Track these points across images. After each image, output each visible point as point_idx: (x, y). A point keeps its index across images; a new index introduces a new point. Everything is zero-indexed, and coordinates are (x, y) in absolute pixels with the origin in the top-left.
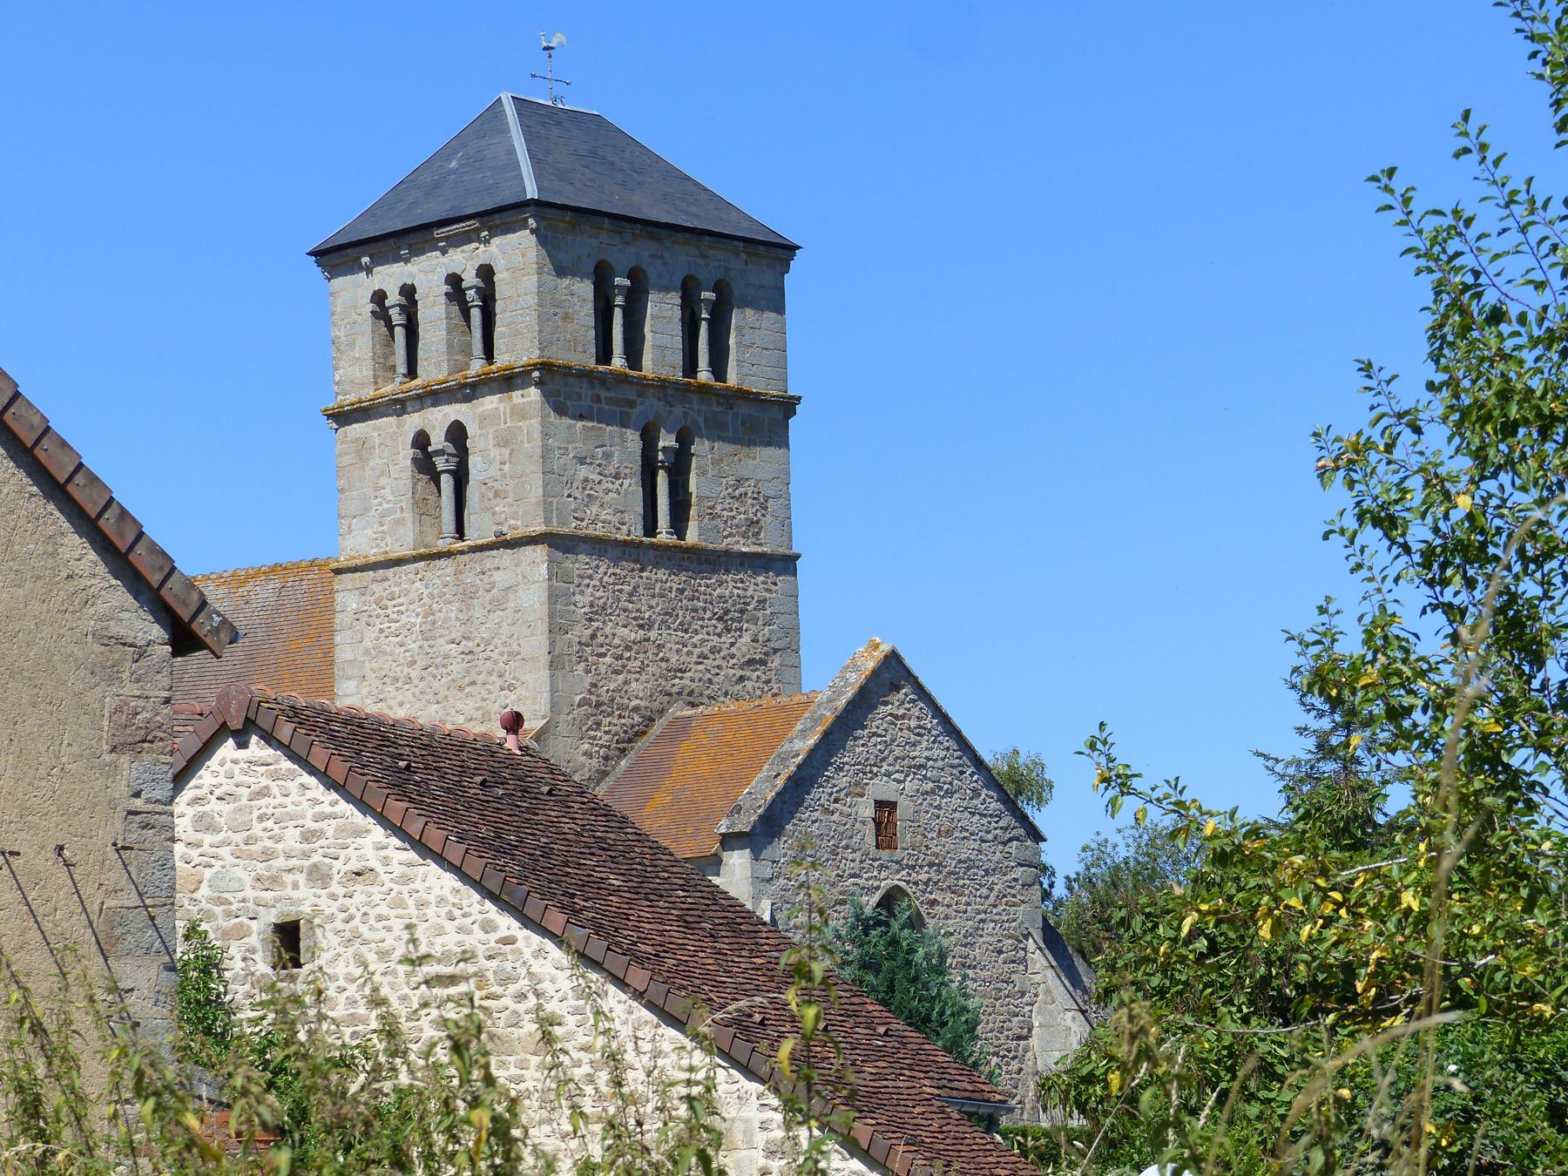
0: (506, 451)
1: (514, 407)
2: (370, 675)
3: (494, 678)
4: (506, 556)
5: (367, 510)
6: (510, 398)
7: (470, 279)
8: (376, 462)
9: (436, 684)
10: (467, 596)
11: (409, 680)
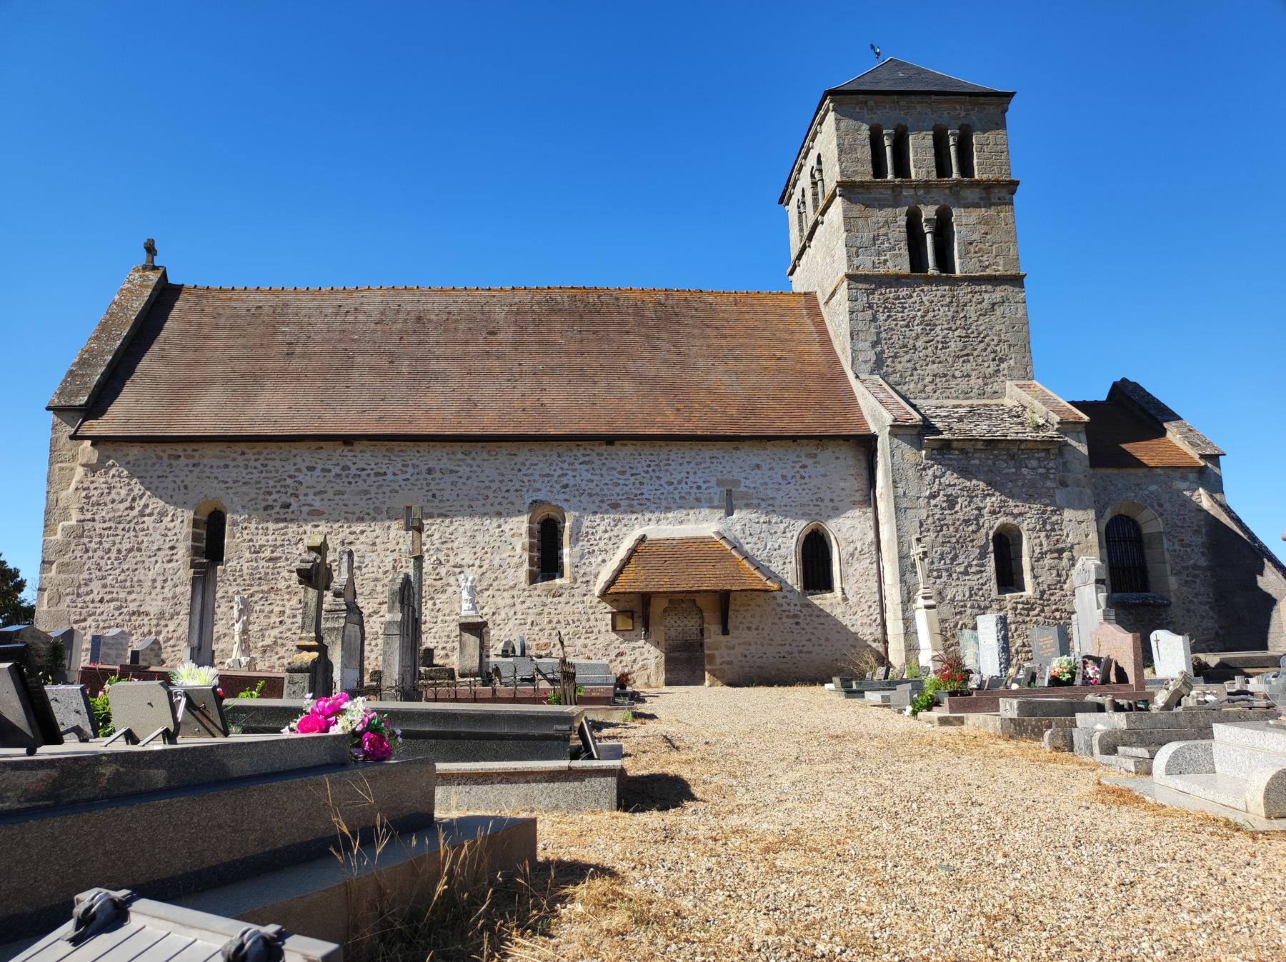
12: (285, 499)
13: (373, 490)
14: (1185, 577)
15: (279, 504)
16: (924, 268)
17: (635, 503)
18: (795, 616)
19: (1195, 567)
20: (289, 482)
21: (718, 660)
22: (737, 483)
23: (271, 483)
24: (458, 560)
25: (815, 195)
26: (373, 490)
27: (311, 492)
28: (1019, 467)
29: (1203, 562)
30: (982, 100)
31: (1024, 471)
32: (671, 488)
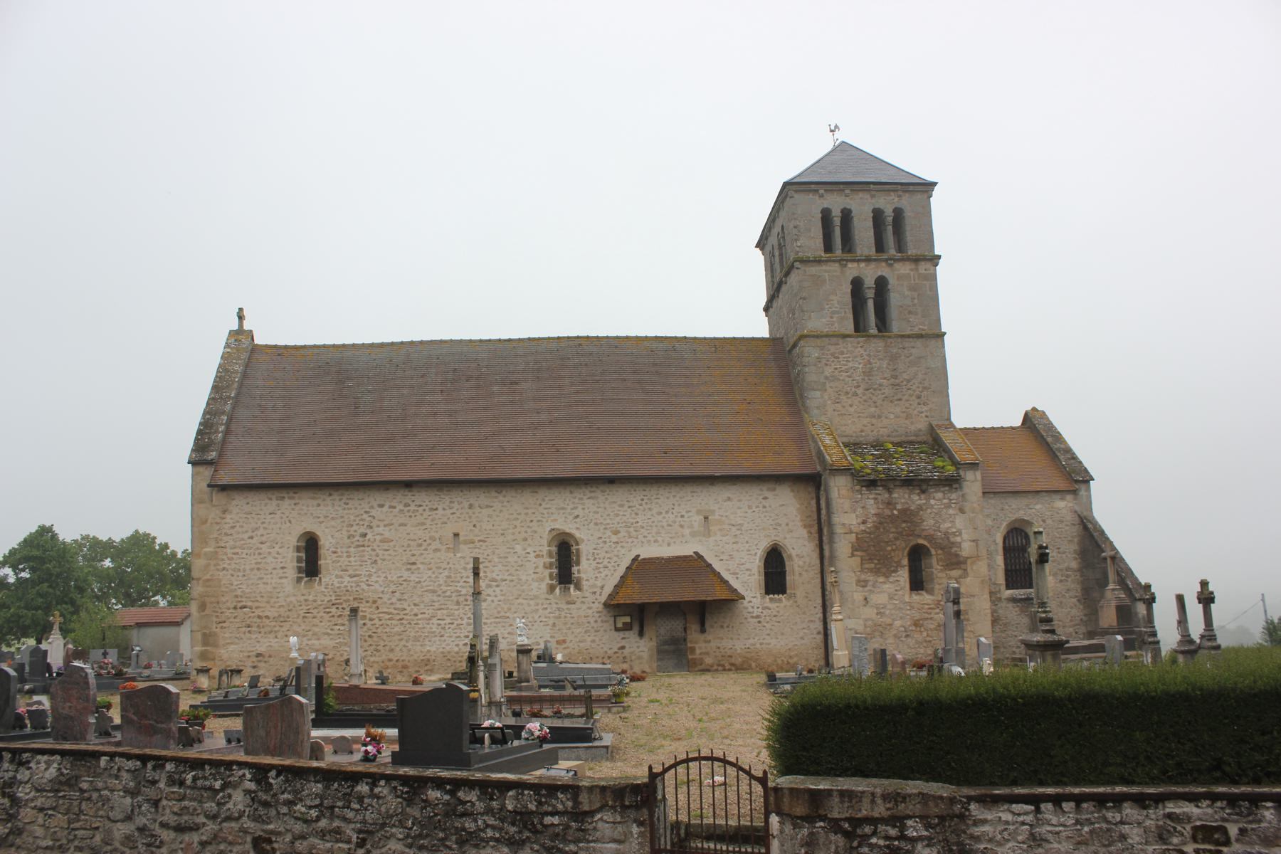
0: (915, 294)
2: (829, 390)
4: (919, 343)
5: (823, 309)
7: (889, 211)
10: (894, 358)
11: (856, 394)
12: (362, 530)
13: (428, 522)
14: (1060, 578)
16: (865, 330)
18: (758, 617)
19: (1068, 569)
20: (365, 516)
21: (698, 651)
22: (713, 512)
23: (352, 518)
24: (494, 575)
25: (781, 255)
26: (428, 522)
27: (382, 524)
28: (928, 499)
29: (1074, 565)
30: (911, 188)
31: (932, 502)
32: (660, 518)
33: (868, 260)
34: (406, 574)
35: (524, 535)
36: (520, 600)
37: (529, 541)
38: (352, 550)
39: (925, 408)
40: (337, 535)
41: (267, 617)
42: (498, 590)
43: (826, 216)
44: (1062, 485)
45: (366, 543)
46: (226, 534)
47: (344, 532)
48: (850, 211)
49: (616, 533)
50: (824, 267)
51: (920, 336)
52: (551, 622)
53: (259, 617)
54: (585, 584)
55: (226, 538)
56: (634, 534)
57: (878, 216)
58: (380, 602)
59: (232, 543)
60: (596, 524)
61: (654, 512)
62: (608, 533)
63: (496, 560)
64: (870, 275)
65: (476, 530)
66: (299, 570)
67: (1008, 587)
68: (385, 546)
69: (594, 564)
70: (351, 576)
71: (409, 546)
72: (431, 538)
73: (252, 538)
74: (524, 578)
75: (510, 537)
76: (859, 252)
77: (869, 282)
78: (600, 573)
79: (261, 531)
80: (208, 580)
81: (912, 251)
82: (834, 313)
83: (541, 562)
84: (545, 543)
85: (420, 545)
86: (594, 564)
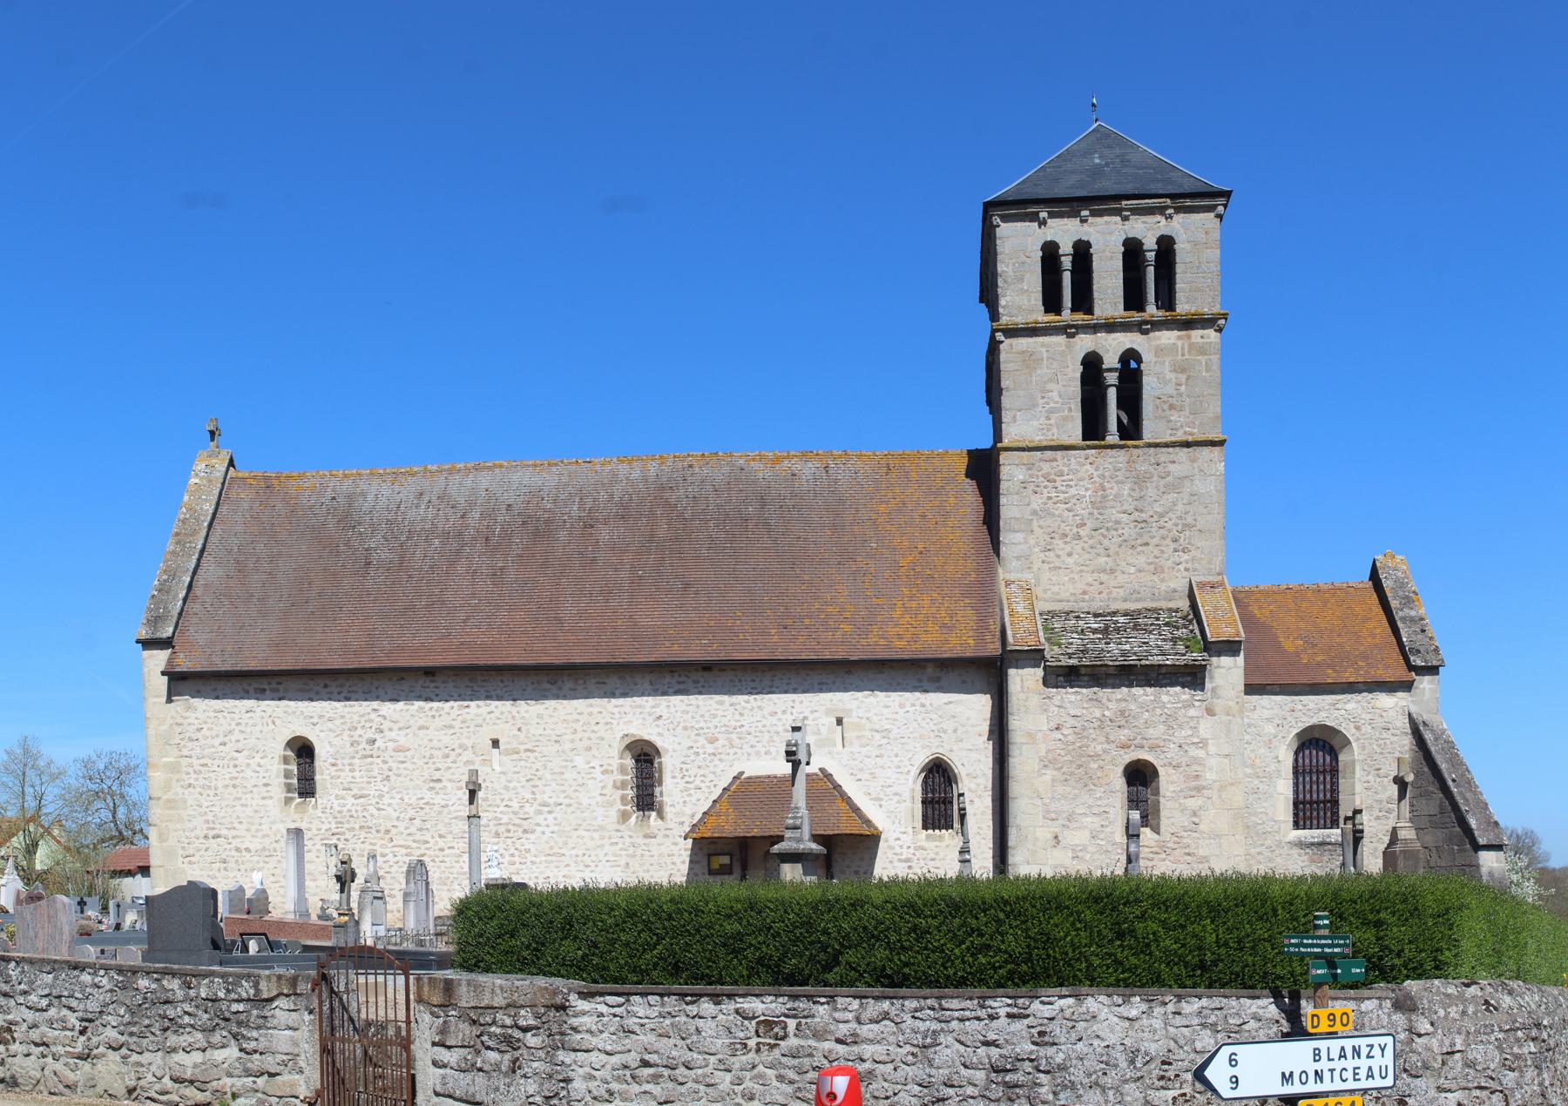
0: (1183, 378)
1: (1191, 346)
3: (1168, 541)
5: (1035, 406)
6: (1189, 337)
7: (1150, 243)
8: (1043, 371)
9: (1106, 542)
10: (1141, 480)
12: (370, 734)
13: (457, 724)
15: (364, 740)
17: (734, 736)
20: (373, 716)
23: (356, 718)
24: (546, 798)
26: (457, 724)
27: (395, 727)
33: (1111, 327)
34: (428, 796)
35: (586, 743)
36: (581, 832)
37: (594, 751)
38: (356, 761)
39: (1186, 557)
40: (335, 741)
41: (248, 850)
42: (550, 817)
43: (1050, 253)
44: (1398, 672)
45: (375, 753)
46: (190, 739)
47: (345, 737)
48: (1088, 245)
49: (712, 741)
50: (1040, 339)
51: (1187, 444)
52: (623, 862)
53: (238, 850)
54: (667, 809)
55: (190, 744)
56: (737, 742)
57: (1132, 250)
58: (394, 831)
59: (198, 751)
60: (685, 728)
61: (766, 712)
62: (702, 740)
63: (548, 776)
64: (1111, 347)
65: (522, 736)
66: (289, 788)
67: (1297, 825)
68: (401, 756)
69: (682, 784)
70: (356, 797)
71: (431, 757)
72: (461, 746)
73: (224, 744)
74: (585, 801)
75: (568, 746)
76: (1097, 311)
77: (1111, 360)
78: (688, 796)
79: (236, 736)
80: (169, 801)
81: (1183, 307)
82: (1051, 411)
83: (609, 780)
84: (615, 753)
85: (447, 756)
86: (682, 784)
